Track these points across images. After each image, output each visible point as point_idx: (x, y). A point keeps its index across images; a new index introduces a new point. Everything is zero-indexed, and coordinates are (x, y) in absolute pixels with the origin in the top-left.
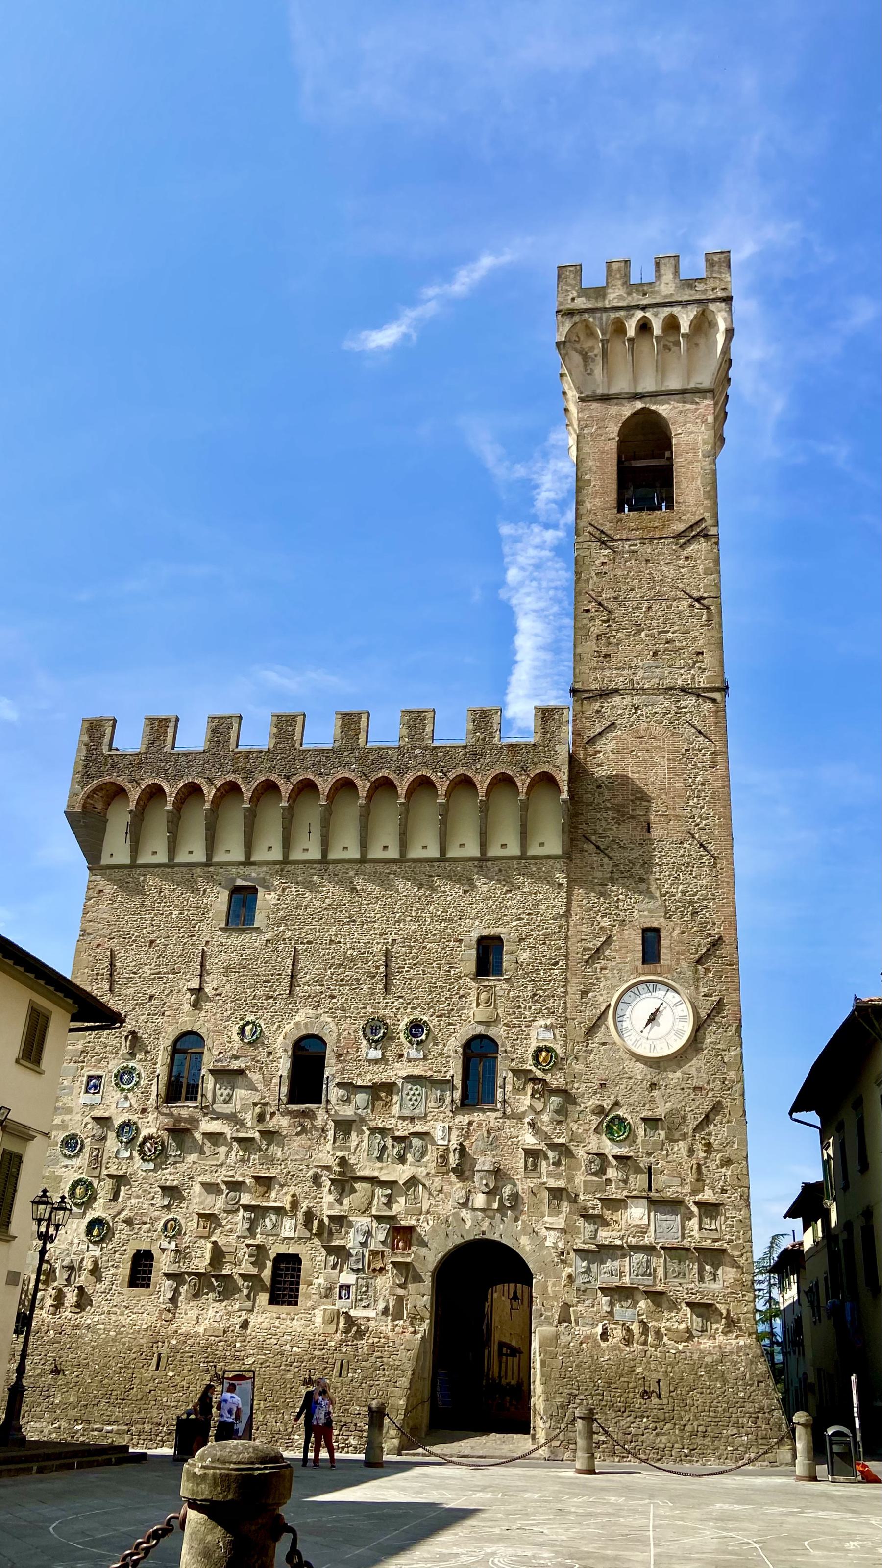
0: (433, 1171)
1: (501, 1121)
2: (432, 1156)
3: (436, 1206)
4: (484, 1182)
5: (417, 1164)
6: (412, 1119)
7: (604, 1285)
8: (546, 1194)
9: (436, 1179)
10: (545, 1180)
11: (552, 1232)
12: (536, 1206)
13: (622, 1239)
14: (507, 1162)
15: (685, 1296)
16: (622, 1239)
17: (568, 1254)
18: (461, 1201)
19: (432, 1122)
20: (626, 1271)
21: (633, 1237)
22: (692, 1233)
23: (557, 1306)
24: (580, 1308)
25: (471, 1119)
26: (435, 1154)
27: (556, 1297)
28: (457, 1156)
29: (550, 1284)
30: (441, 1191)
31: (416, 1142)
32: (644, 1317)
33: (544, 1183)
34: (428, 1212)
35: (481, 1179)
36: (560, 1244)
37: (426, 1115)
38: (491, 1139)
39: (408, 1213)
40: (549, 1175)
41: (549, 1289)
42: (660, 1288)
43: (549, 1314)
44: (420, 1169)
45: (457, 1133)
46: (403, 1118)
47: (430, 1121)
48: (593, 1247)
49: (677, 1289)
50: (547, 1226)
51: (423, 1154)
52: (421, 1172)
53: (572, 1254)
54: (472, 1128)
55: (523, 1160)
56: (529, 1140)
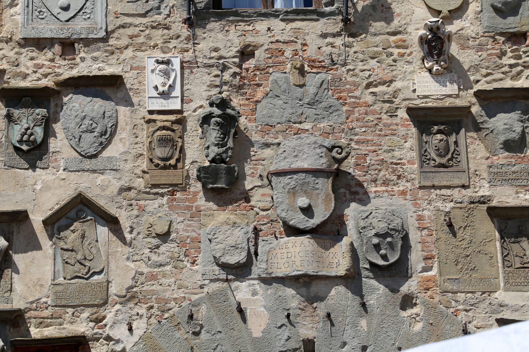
0: (140, 183)
1: (338, 41)
2: (129, 147)
3: (153, 277)
4: (303, 201)
5: (88, 164)
6: (68, 46)
8: (488, 229)
9: (152, 205)
10: (485, 191)
12: (465, 262)
14: (364, 149)
18: (233, 259)
19: (129, 53)
25: (249, 39)
26: (143, 135)
28: (214, 134)
30: (164, 237)
31: (75, 104)
33: (482, 201)
34: (130, 297)
35: (293, 192)
37: (109, 34)
38: (311, 90)
39: (63, 304)
40: (497, 177)
44: (100, 179)
45: (208, 79)
46: (40, 44)
47: (122, 49)
51: (108, 136)
52: (101, 188)
54: (250, 64)
55: (412, 142)
56: (425, 86)
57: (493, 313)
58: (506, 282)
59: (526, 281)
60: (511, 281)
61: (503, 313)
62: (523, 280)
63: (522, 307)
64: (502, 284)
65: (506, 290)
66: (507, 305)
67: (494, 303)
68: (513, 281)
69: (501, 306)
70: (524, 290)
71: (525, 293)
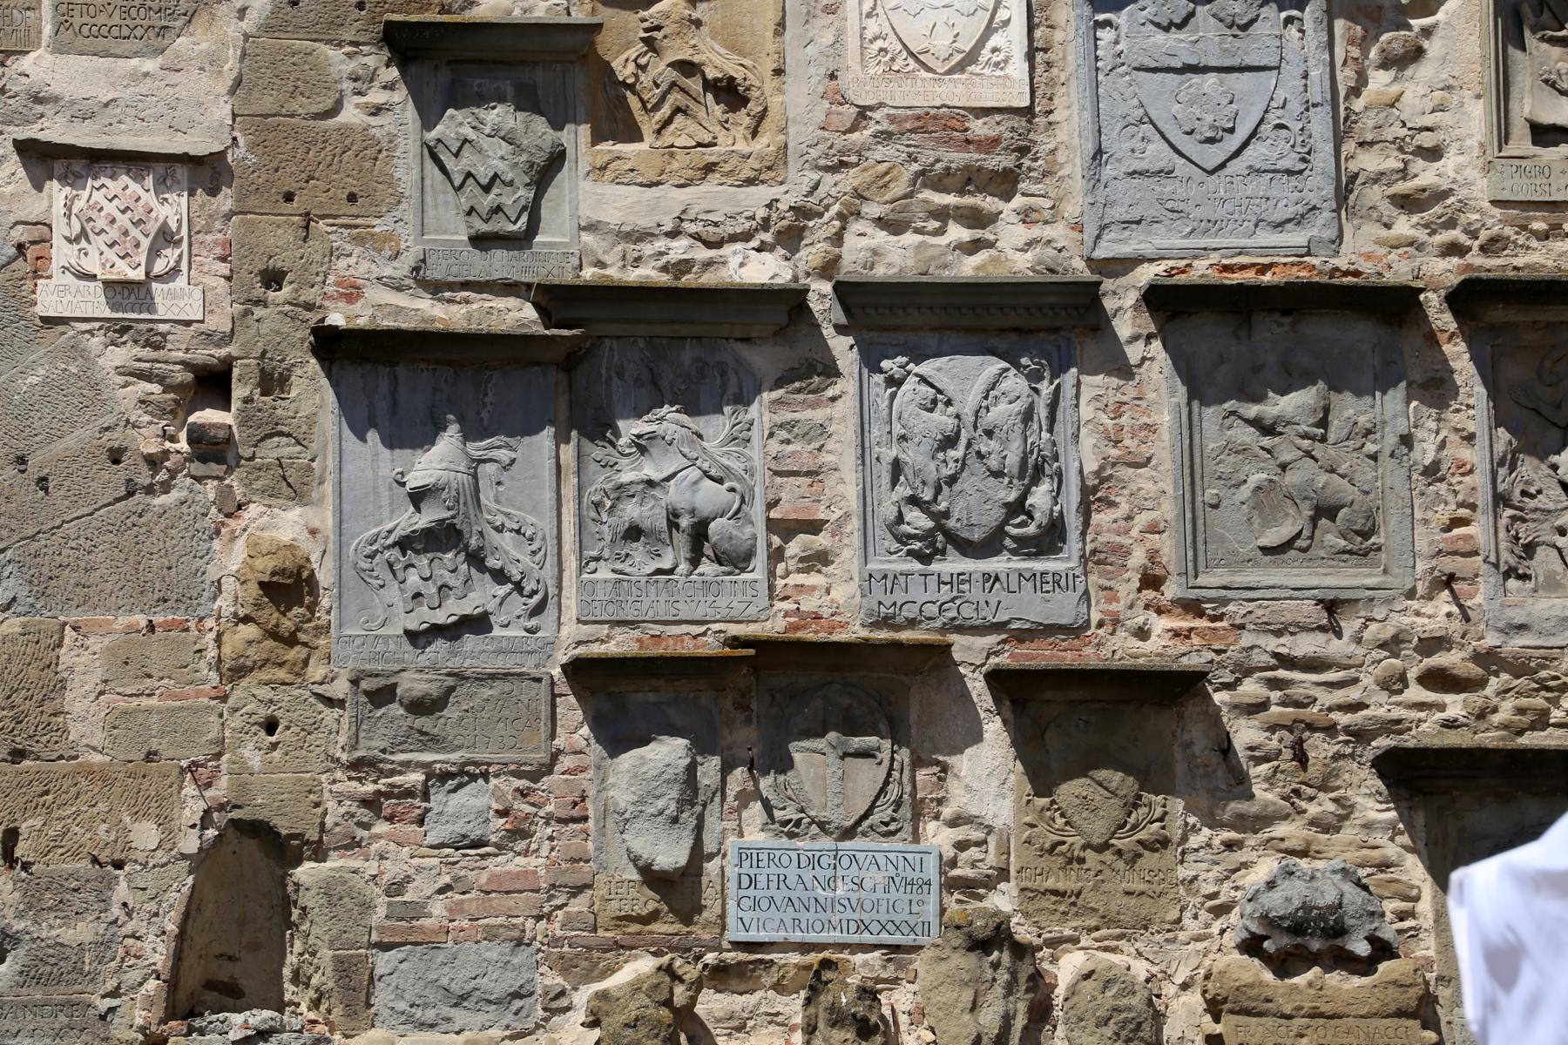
7: (620, 644)
11: (113, 195)
13: (790, 239)
15: (1381, 707)
16: (790, 239)
17: (272, 382)
20: (816, 503)
21: (892, 226)
22: (1426, 175)
23: (164, 842)
24: (395, 854)
27: (143, 776)
29: (83, 663)
32: (1003, 900)
36: (178, 301)
41: (78, 701)
42: (1156, 642)
43: (83, 931)
48: (519, 315)
49: (1304, 645)
50: (55, 131)
53: (313, 393)
57: (10, 123)
58: (62, 25)
59: (128, 21)
60: (77, 21)
61: (44, 122)
62: (116, 20)
63: (106, 105)
64: (47, 30)
65: (59, 49)
66: (57, 99)
67: (15, 89)
68: (86, 19)
69: (38, 99)
70: (118, 52)
71: (121, 62)
